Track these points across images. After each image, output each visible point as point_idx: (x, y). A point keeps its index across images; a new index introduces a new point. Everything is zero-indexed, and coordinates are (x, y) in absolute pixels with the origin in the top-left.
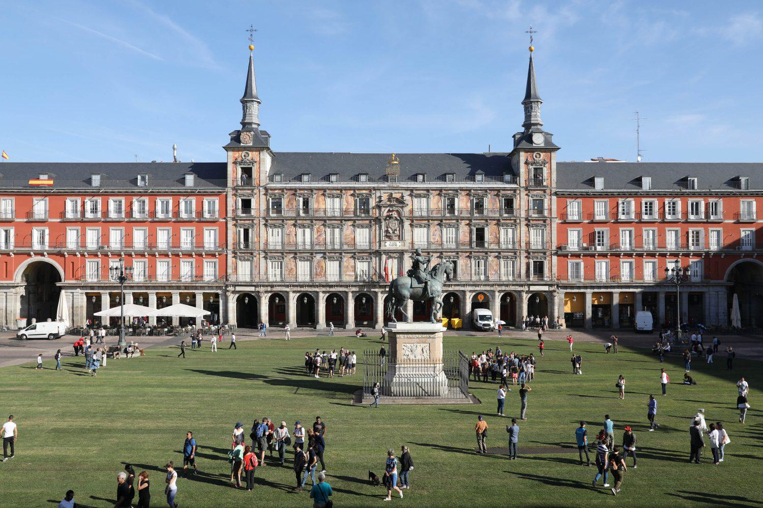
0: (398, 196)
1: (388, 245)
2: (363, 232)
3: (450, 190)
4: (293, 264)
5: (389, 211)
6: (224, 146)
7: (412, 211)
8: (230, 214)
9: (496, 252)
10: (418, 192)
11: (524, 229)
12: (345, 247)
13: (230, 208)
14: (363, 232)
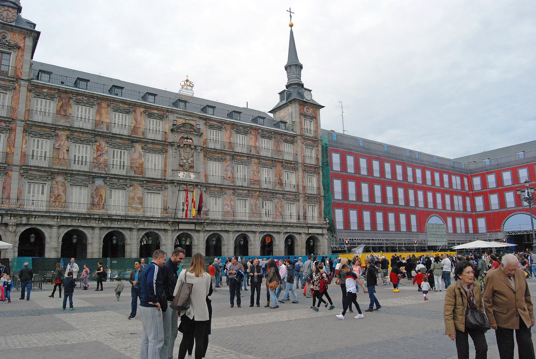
1: (181, 175)
2: (152, 158)
3: (241, 126)
4: (61, 189)
5: (182, 137)
7: (205, 143)
9: (281, 194)
10: (212, 123)
11: (300, 173)
12: (132, 174)
14: (152, 158)
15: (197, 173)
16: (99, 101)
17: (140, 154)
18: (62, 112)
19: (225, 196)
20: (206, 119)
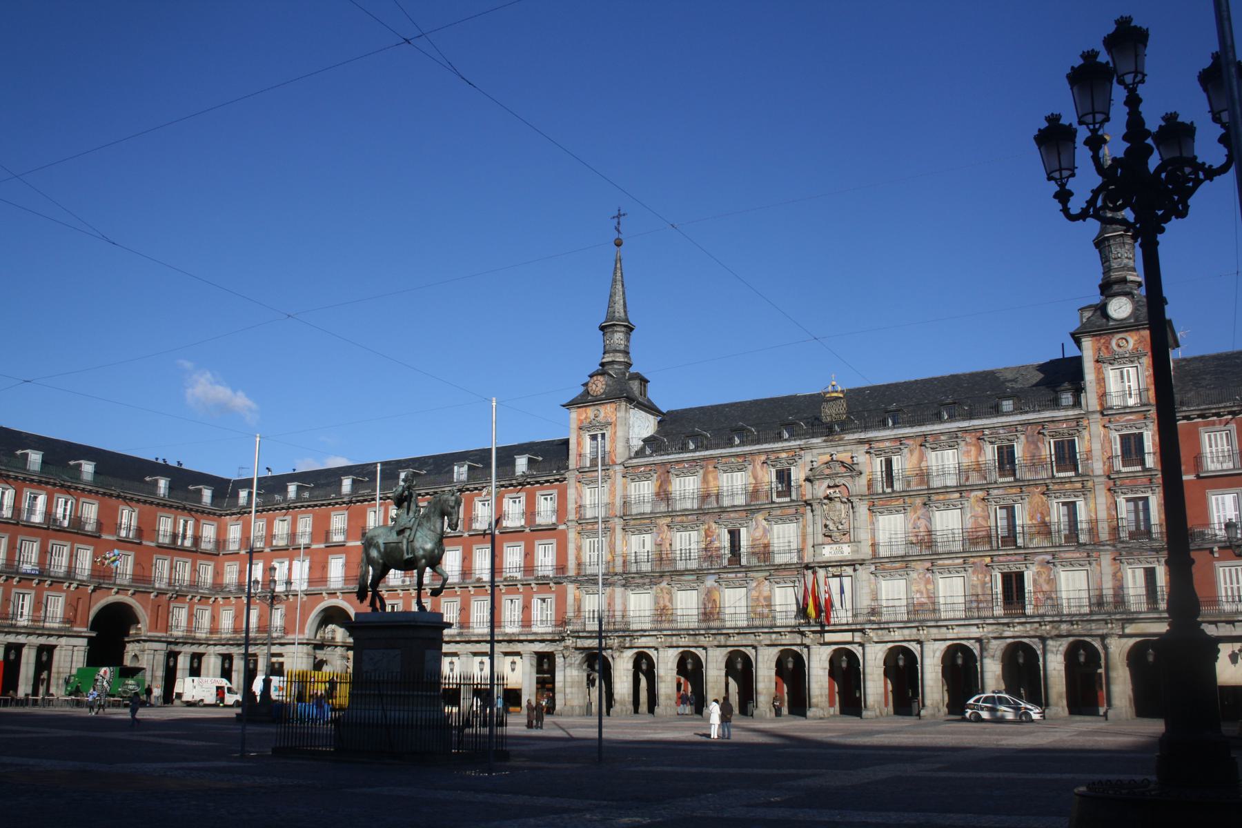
0: (845, 457)
1: (829, 552)
3: (942, 434)
4: (667, 597)
6: (564, 403)
8: (572, 516)
10: (881, 445)
13: (571, 506)
15: (855, 542)
16: (704, 463)
17: (765, 529)
18: (663, 495)
19: (914, 575)
20: (869, 442)
